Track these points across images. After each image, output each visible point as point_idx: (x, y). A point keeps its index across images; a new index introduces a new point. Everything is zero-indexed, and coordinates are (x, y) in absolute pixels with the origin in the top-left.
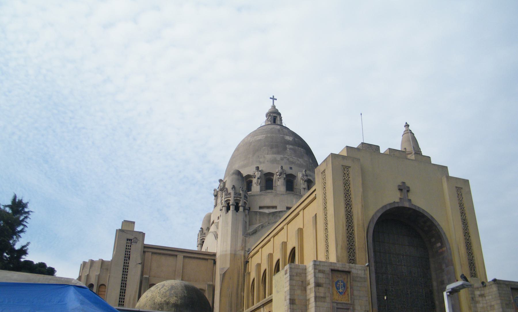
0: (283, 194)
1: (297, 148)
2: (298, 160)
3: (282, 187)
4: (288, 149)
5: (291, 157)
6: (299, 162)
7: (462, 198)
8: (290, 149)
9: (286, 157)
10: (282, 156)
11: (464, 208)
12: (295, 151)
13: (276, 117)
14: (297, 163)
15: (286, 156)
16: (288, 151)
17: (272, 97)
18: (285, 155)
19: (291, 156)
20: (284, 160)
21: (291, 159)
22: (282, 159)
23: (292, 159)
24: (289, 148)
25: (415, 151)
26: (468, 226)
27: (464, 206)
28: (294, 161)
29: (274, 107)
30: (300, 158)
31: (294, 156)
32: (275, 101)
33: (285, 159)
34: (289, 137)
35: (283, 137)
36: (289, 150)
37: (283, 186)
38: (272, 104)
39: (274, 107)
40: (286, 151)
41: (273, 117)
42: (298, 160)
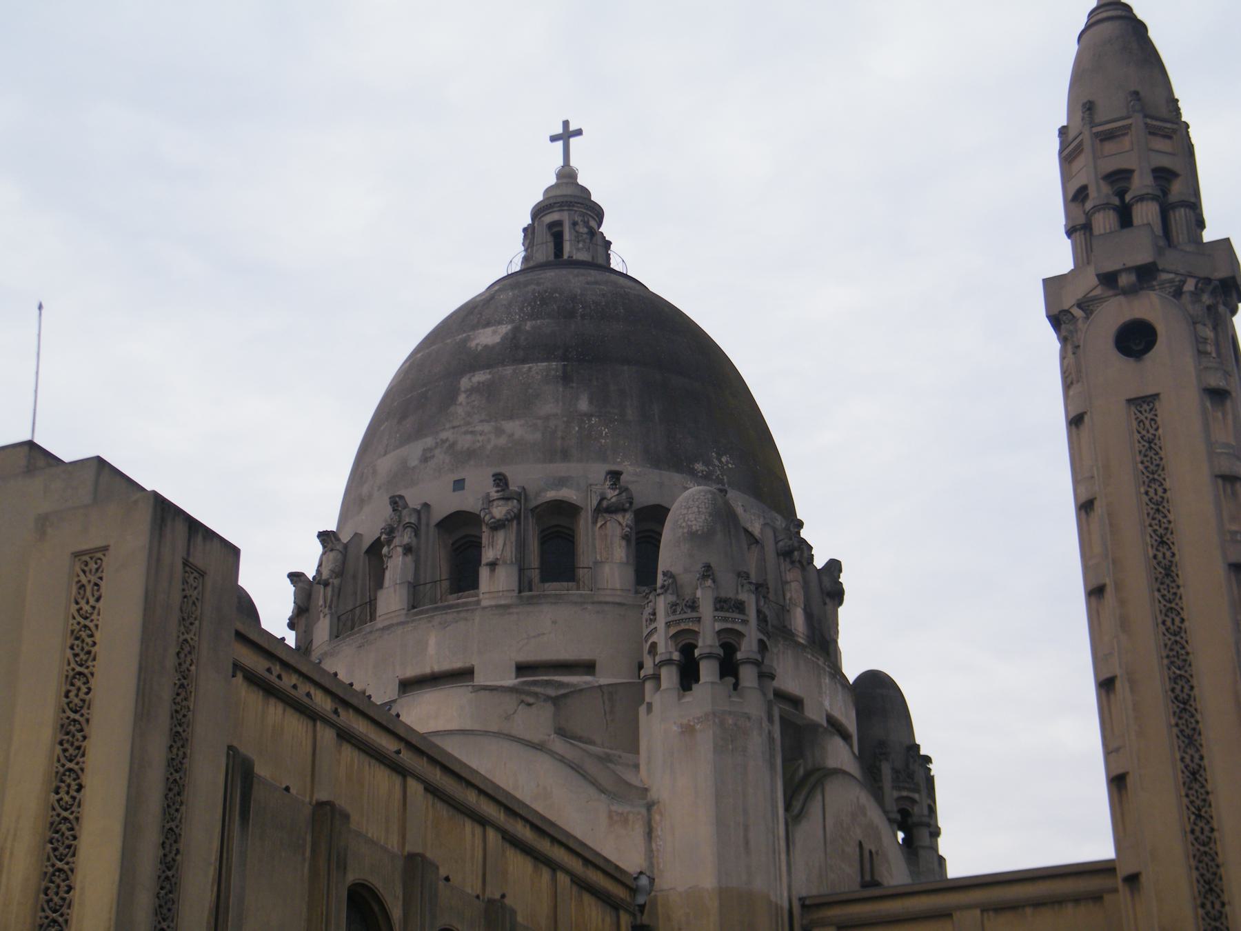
0: (506, 607)
1: (509, 370)
2: (499, 432)
3: (395, 591)
4: (462, 398)
5: (466, 433)
6: (502, 441)
7: (98, 600)
8: (472, 391)
9: (447, 440)
10: (429, 441)
11: (94, 644)
12: (488, 391)
13: (559, 223)
14: (489, 447)
15: (444, 435)
16: (461, 404)
17: (572, 127)
18: (444, 429)
19: (468, 424)
20: (434, 456)
21: (465, 442)
22: (425, 459)
23: (469, 437)
24: (465, 392)
25: (1093, 124)
26: (85, 738)
27: (98, 636)
28: (478, 445)
29: (567, 175)
30: (511, 418)
31: (482, 421)
32: (573, 141)
33: (437, 452)
34: (489, 330)
35: (465, 341)
36: (467, 397)
37: (398, 587)
38: (561, 163)
39: (567, 175)
40: (452, 409)
41: (545, 229)
42: (499, 432)
